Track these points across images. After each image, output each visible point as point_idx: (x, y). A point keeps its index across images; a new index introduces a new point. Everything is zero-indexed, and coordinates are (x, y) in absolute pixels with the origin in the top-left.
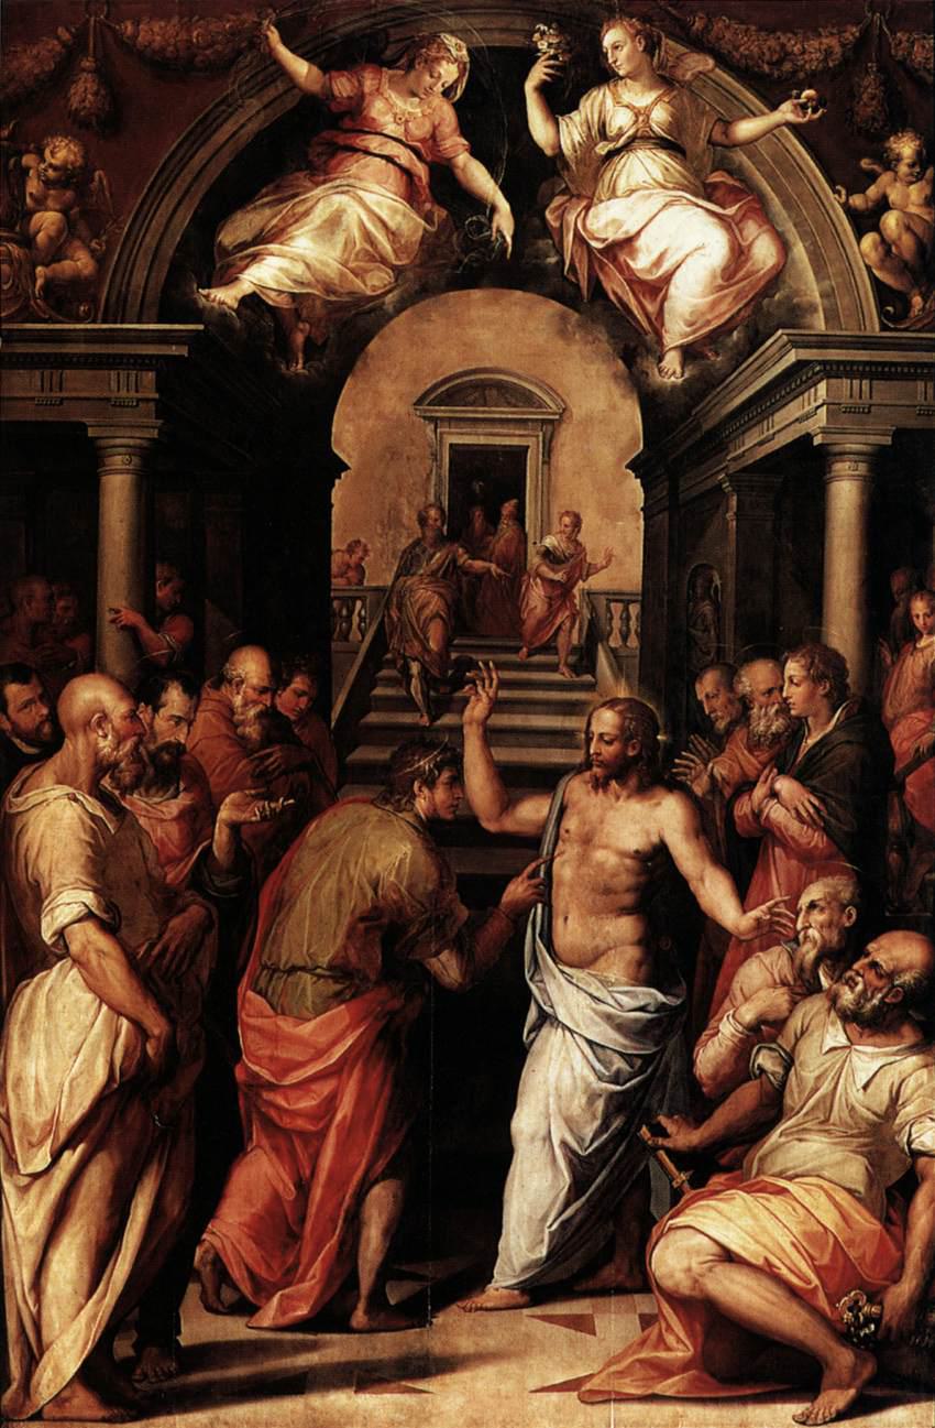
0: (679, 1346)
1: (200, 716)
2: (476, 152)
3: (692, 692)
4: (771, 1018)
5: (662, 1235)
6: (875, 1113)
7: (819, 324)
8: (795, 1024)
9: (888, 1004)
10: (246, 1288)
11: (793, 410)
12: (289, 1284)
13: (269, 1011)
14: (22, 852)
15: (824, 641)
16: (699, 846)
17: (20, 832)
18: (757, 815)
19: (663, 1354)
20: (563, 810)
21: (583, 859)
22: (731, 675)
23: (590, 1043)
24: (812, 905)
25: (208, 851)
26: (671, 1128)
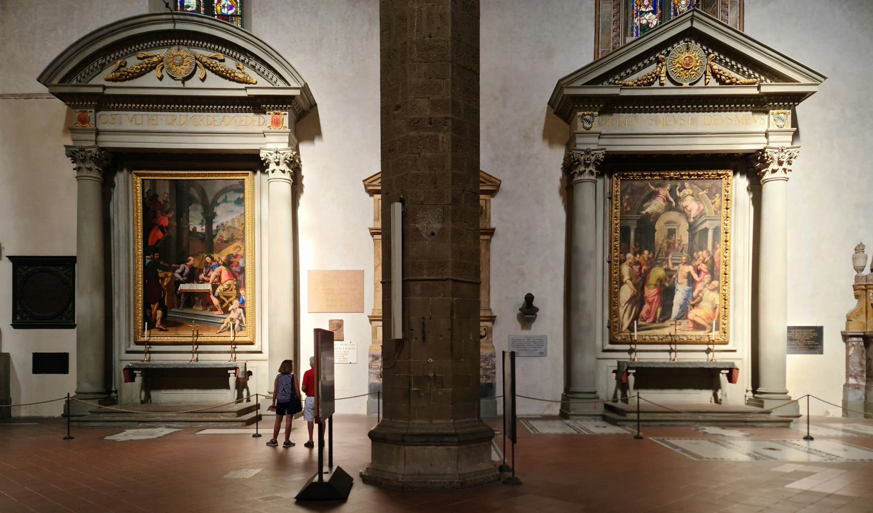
0: (691, 325)
2: (671, 196)
7: (708, 215)
11: (705, 224)
20: (679, 268)
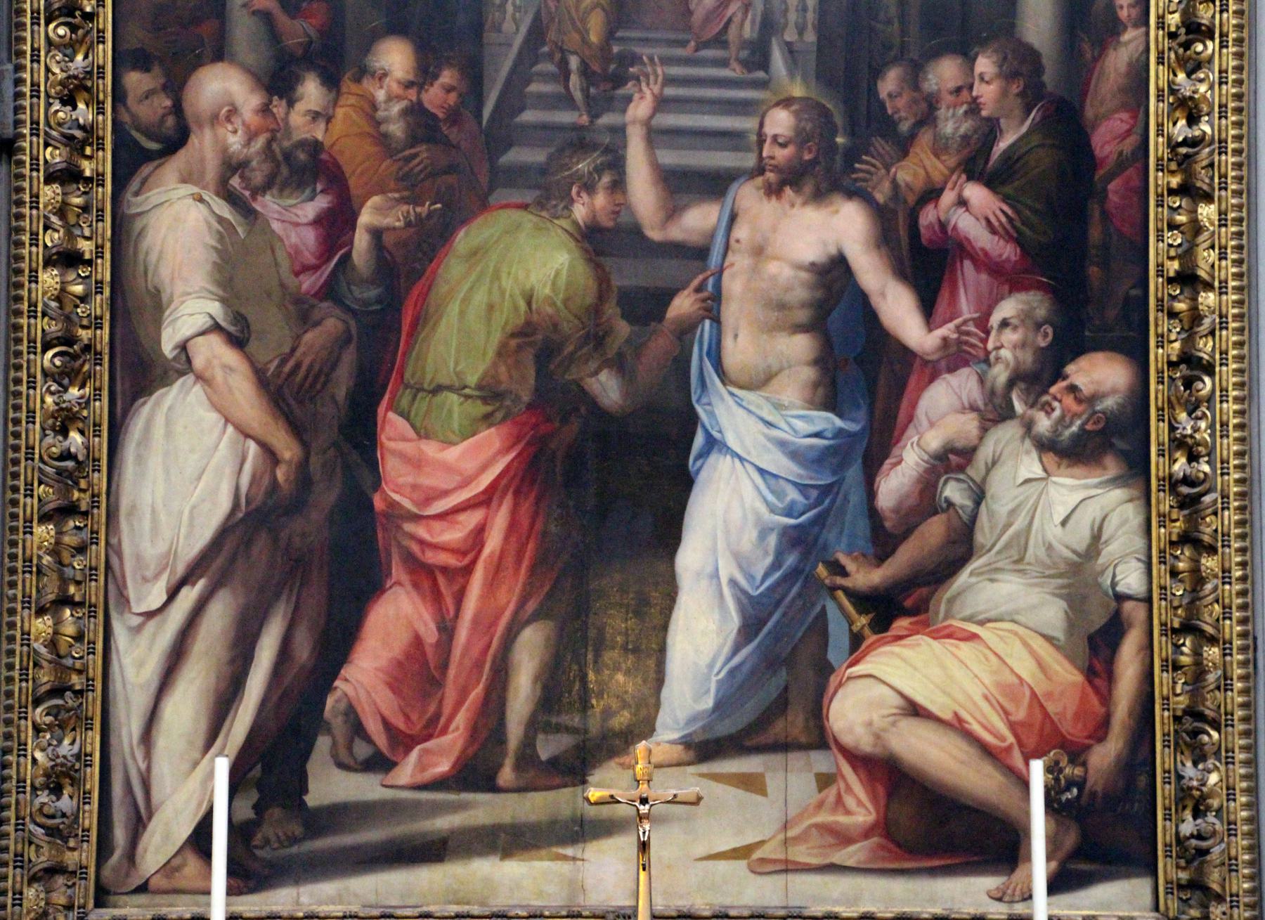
1: (340, 112)
3: (873, 91)
4: (959, 444)
5: (840, 685)
6: (1074, 552)
8: (985, 453)
9: (1090, 432)
10: (381, 740)
12: (429, 737)
13: (411, 433)
14: (141, 257)
15: (1018, 36)
16: (881, 257)
17: (140, 234)
18: (943, 225)
19: (842, 819)
20: (733, 218)
21: (755, 270)
22: (916, 72)
23: (762, 472)
24: (1005, 324)
25: (347, 257)
26: (850, 566)
